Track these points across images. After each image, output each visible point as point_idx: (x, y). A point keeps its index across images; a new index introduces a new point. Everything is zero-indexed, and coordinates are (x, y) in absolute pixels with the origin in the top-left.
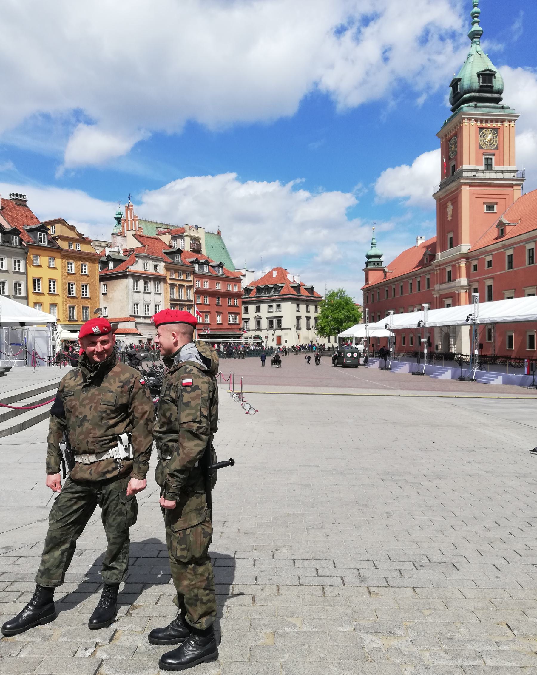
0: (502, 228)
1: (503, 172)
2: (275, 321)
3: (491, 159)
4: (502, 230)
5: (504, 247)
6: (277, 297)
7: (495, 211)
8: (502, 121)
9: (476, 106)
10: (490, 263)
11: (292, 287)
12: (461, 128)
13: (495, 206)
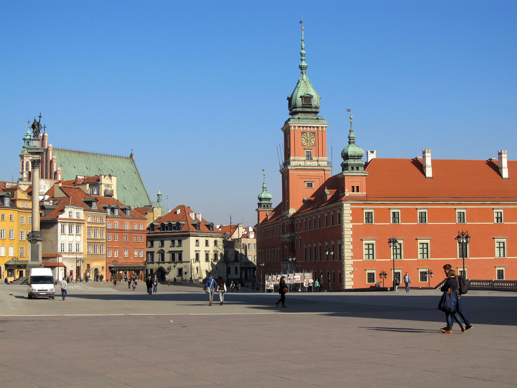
2: (177, 256)
6: (178, 234)
8: (317, 127)
11: (192, 225)
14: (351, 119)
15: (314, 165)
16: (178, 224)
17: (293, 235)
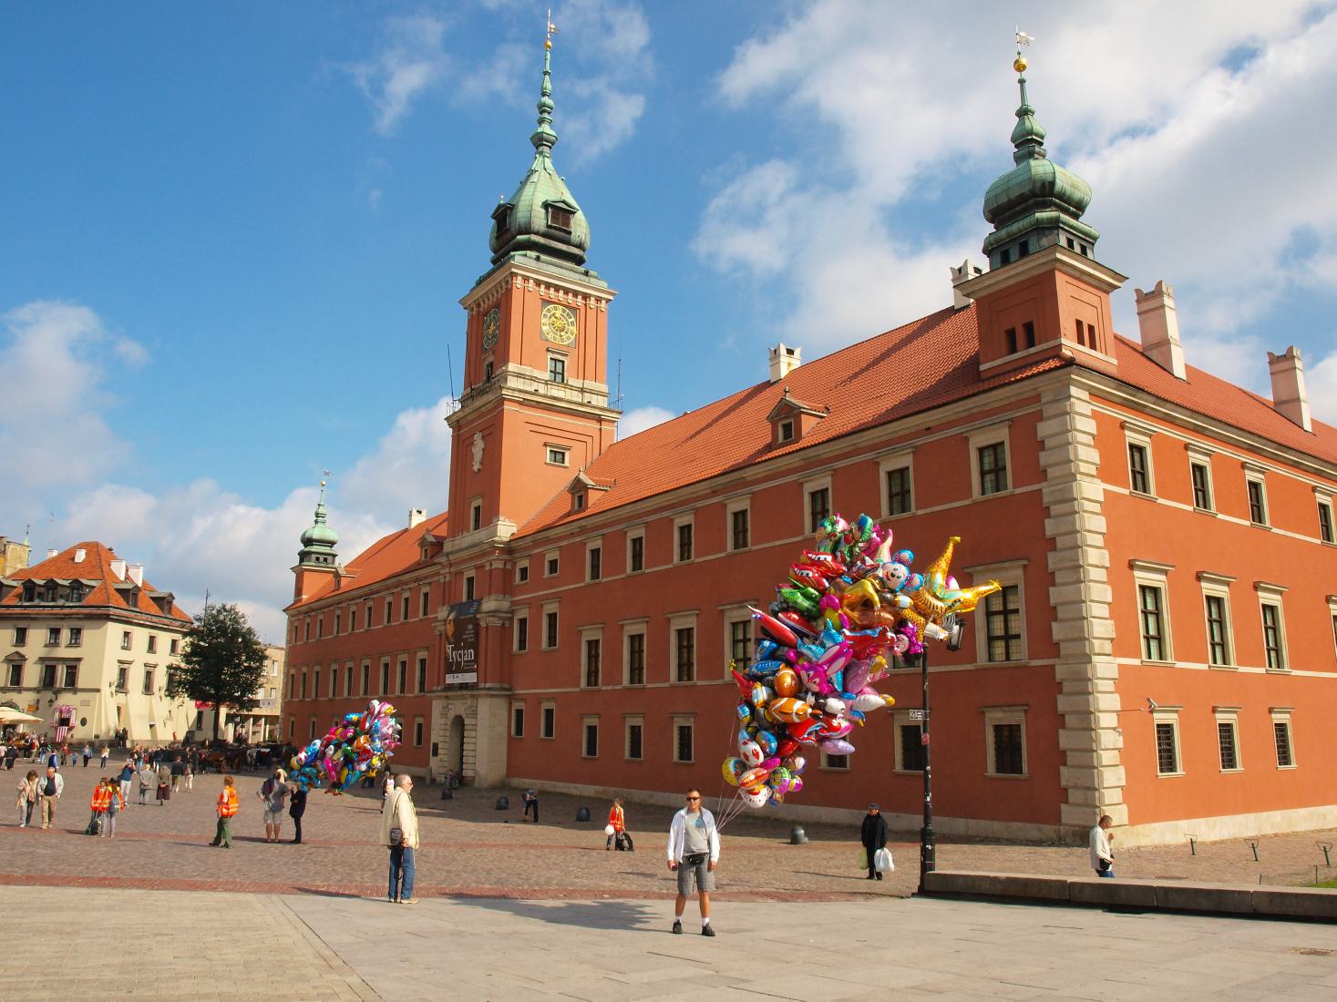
0: (580, 494)
1: (582, 390)
2: (61, 672)
3: (563, 362)
4: (580, 498)
5: (583, 530)
6: (74, 610)
7: (567, 463)
8: (586, 297)
9: (538, 259)
10: (553, 564)
11: (117, 590)
12: (509, 292)
13: (567, 454)
14: (1020, 67)
15: (575, 399)
16: (77, 585)
17: (505, 605)
